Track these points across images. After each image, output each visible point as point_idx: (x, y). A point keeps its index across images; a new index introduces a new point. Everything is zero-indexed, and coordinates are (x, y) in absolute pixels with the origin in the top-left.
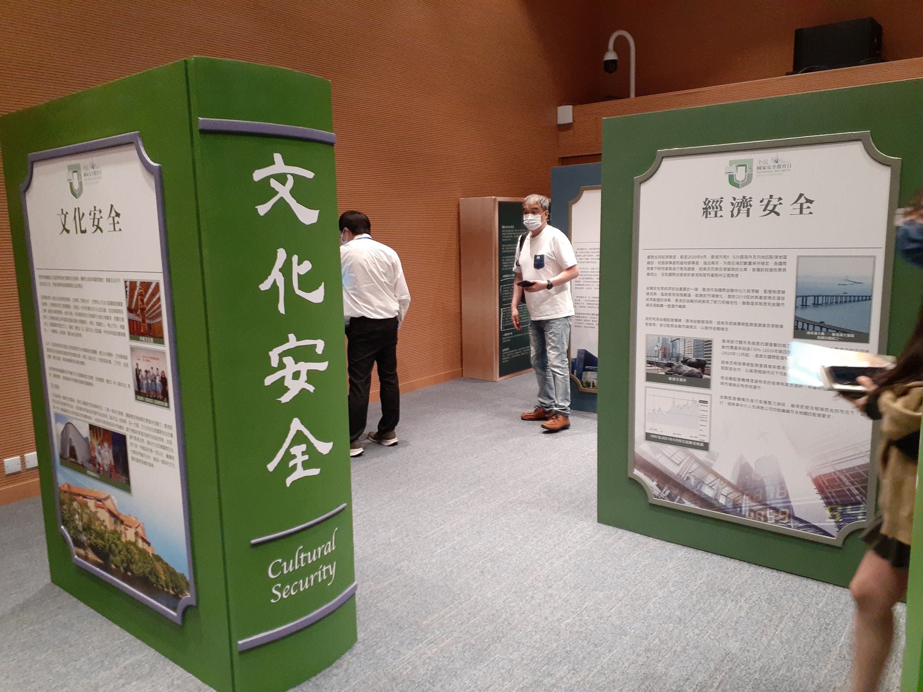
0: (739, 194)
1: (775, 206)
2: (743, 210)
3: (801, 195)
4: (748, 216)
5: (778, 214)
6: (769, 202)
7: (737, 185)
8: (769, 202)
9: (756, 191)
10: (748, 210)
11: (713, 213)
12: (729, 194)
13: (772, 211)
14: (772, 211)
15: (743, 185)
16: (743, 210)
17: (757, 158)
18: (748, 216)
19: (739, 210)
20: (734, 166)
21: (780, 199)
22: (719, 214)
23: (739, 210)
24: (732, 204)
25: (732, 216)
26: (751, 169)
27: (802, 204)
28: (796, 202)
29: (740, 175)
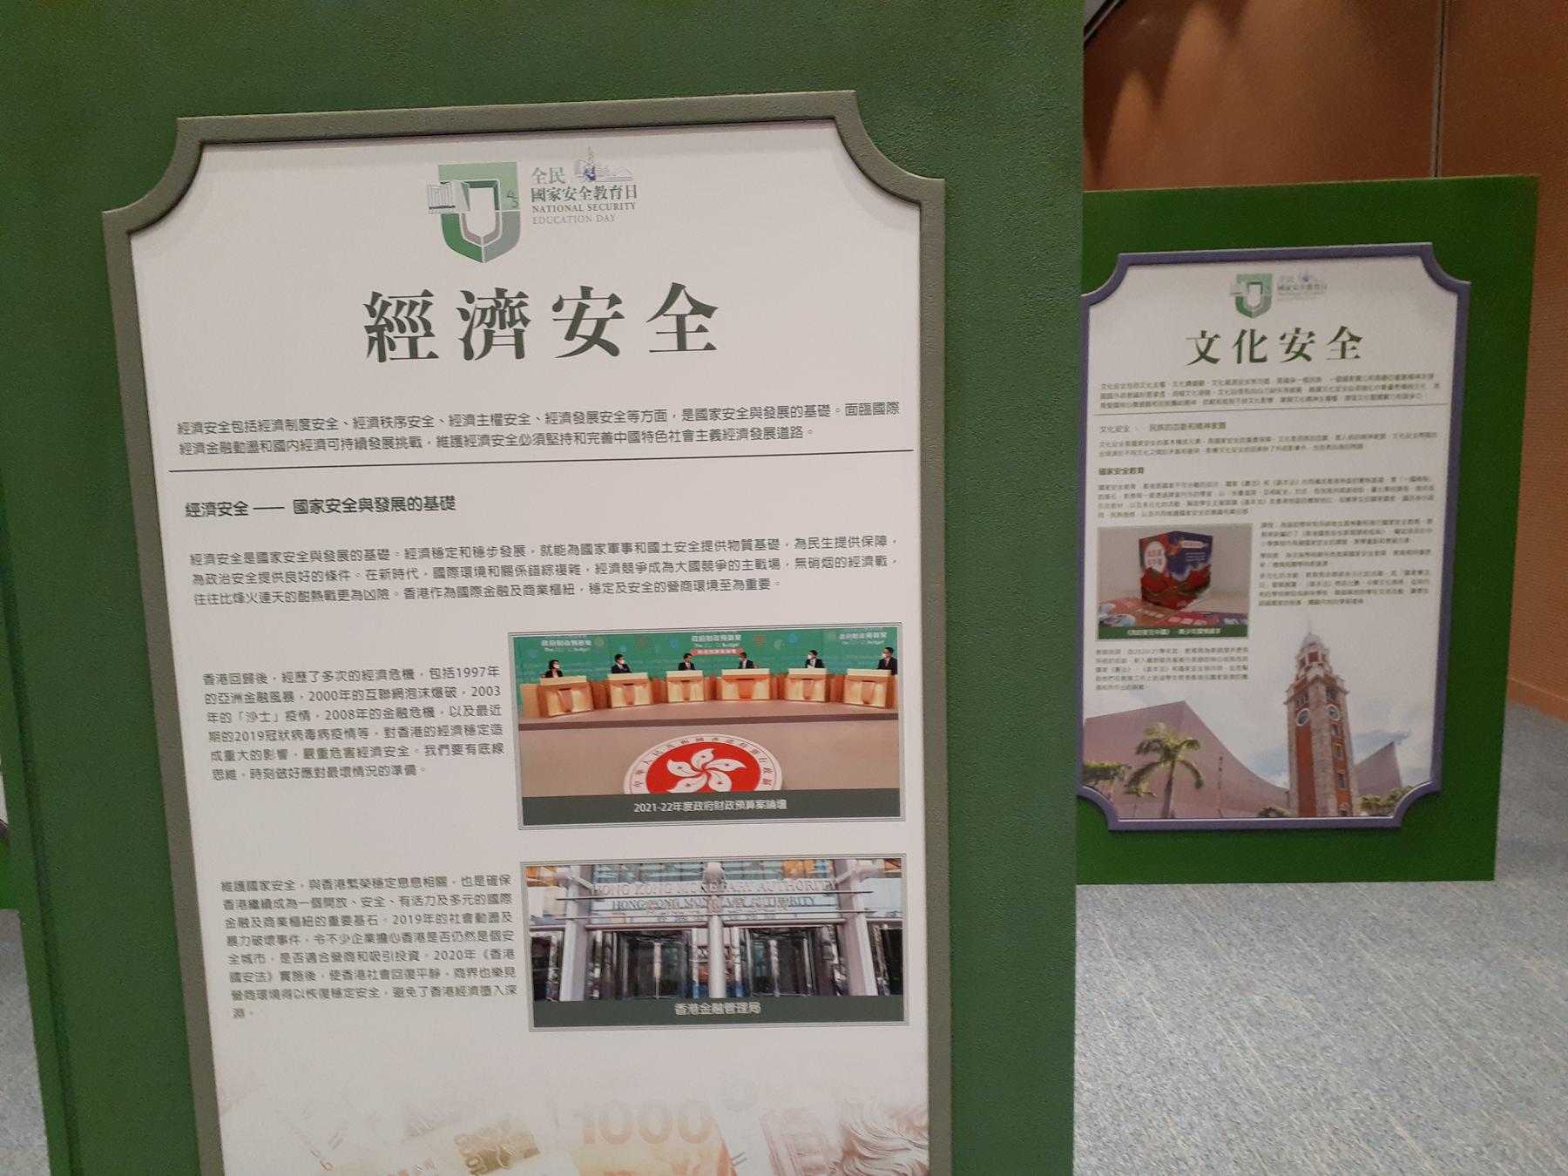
0: (484, 279)
1: (601, 324)
2: (504, 336)
3: (676, 290)
4: (520, 354)
5: (613, 350)
6: (581, 309)
7: (473, 252)
8: (581, 309)
9: (539, 270)
10: (518, 335)
11: (403, 347)
12: (451, 280)
13: (595, 339)
14: (595, 339)
15: (494, 252)
16: (504, 336)
17: (533, 160)
18: (520, 354)
19: (489, 336)
20: (455, 186)
21: (614, 300)
22: (424, 346)
23: (489, 336)
24: (465, 314)
25: (469, 354)
26: (512, 196)
27: (681, 319)
28: (661, 312)
29: (480, 219)
